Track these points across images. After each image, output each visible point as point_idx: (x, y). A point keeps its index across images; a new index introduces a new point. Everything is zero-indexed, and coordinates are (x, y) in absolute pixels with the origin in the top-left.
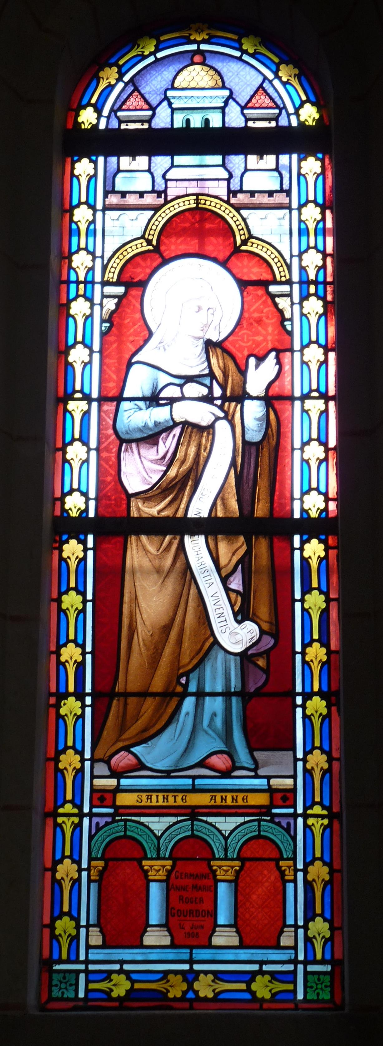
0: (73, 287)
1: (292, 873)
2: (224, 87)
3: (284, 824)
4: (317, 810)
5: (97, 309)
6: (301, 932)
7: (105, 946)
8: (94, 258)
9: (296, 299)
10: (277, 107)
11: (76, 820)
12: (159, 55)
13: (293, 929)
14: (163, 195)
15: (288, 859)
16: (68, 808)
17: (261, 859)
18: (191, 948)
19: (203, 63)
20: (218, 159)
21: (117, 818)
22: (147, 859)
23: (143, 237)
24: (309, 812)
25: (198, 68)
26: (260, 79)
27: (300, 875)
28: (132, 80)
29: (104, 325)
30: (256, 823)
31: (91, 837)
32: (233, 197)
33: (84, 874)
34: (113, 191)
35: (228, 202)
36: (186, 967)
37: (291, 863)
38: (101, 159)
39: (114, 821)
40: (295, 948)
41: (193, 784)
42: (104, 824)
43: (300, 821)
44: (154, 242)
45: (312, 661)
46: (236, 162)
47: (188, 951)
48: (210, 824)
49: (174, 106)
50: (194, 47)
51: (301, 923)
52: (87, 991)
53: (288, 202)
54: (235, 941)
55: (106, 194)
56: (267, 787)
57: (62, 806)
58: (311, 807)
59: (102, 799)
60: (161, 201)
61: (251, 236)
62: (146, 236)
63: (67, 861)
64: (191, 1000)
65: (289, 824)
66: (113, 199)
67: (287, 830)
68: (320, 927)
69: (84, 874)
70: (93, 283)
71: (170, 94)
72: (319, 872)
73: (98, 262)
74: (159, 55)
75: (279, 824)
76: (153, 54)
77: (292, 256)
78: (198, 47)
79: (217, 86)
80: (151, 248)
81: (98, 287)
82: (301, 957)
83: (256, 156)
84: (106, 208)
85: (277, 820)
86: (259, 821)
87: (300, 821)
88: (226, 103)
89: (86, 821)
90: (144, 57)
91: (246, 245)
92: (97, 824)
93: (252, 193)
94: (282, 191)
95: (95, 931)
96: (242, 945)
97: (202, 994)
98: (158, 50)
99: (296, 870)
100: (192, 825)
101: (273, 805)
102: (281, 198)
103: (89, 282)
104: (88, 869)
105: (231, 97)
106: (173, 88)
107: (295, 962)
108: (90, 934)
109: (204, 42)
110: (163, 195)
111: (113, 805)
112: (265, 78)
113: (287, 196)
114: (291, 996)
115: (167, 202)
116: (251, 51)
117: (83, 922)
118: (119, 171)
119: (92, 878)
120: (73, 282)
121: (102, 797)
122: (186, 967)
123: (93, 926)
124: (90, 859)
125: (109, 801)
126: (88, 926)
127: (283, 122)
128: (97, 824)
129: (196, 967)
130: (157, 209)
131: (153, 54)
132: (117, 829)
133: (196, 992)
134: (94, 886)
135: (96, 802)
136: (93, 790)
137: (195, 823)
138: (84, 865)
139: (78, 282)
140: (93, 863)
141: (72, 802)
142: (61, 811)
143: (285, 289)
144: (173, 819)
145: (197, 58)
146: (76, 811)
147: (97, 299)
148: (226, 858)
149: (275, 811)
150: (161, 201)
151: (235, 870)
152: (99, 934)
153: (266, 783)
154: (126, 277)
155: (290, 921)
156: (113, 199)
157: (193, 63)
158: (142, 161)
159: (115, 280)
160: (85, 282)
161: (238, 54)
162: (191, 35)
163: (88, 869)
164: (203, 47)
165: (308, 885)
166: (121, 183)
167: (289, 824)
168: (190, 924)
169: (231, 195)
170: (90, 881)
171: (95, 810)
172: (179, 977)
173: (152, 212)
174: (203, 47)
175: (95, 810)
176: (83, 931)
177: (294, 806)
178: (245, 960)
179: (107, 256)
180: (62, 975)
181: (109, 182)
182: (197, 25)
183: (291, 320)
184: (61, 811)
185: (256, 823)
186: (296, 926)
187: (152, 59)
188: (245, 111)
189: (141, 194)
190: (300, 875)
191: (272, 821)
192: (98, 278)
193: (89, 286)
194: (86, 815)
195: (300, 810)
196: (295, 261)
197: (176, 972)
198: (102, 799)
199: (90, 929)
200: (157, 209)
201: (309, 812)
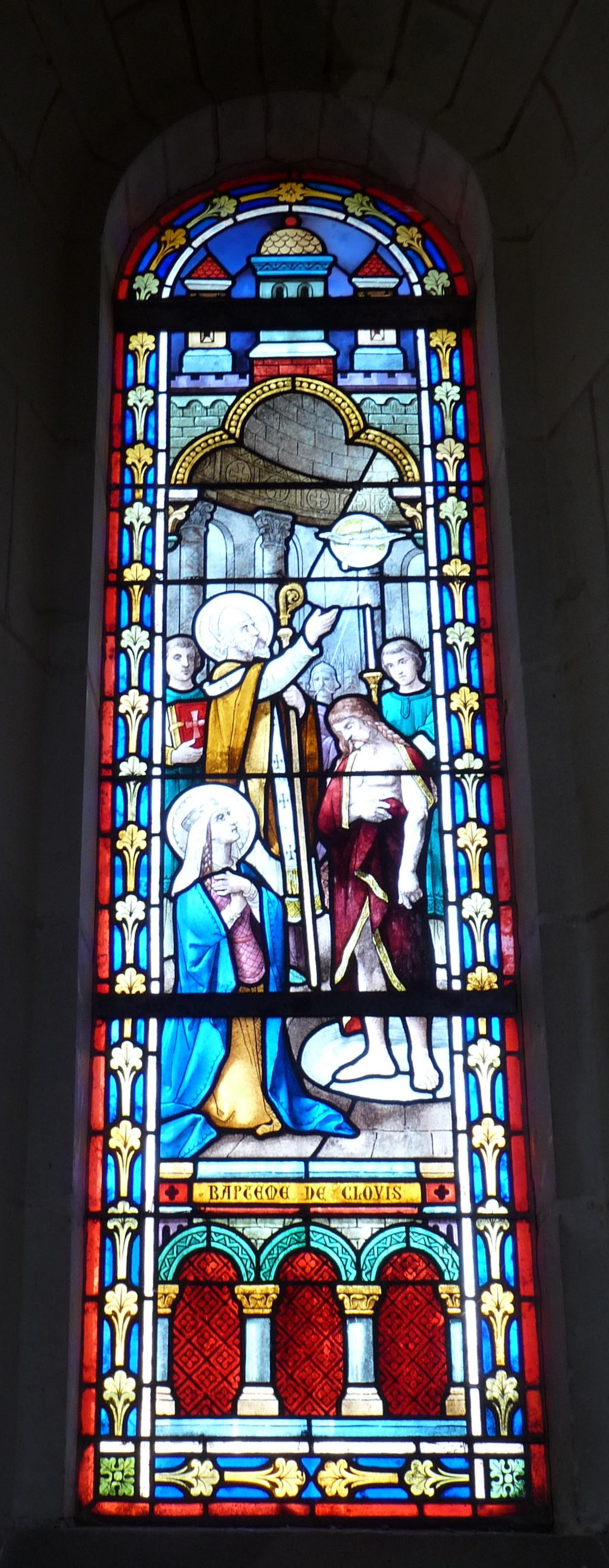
0: (128, 493)
1: (458, 1303)
2: (325, 252)
3: (443, 1228)
4: (492, 1207)
5: (160, 517)
6: (475, 1394)
7: (181, 1413)
8: (156, 451)
9: (430, 500)
10: (394, 275)
11: (133, 1224)
12: (240, 217)
13: (462, 1390)
14: (248, 376)
15: (451, 1282)
16: (123, 1207)
17: (411, 1300)
18: (309, 1418)
19: (298, 226)
20: (319, 334)
21: (195, 1221)
22: (240, 1281)
23: (222, 428)
24: (481, 1210)
25: (291, 232)
26: (372, 244)
27: (470, 1306)
28: (205, 244)
29: (170, 538)
30: (403, 1229)
31: (158, 1251)
32: (342, 377)
33: (148, 1306)
34: (181, 373)
35: (334, 383)
36: (304, 1447)
37: (456, 1289)
38: (164, 336)
39: (191, 1225)
40: (467, 1417)
41: (307, 1171)
42: (176, 1230)
43: (467, 1223)
44: (237, 436)
45: (477, 1066)
46: (344, 339)
47: (305, 1422)
48: (334, 1230)
49: (259, 273)
50: (285, 208)
51: (474, 1379)
52: (154, 1484)
53: (415, 383)
54: (377, 1408)
55: (171, 376)
56: (414, 1176)
57: (114, 1204)
58: (483, 1203)
59: (172, 1193)
60: (245, 383)
61: (367, 426)
62: (227, 427)
63: (121, 1288)
64: (311, 1502)
65: (450, 1229)
66: (183, 382)
67: (448, 1238)
68: (503, 1387)
69: (148, 1306)
70: (155, 486)
71: (254, 260)
72: (498, 1301)
73: (162, 457)
74: (240, 217)
75: (435, 1230)
76: (233, 216)
77: (422, 446)
78: (290, 208)
79: (316, 252)
80: (232, 442)
81: (161, 492)
82: (477, 1431)
83: (368, 332)
84: (172, 392)
85: (431, 1224)
86: (408, 1226)
87: (467, 1223)
88: (329, 270)
89: (149, 1222)
90: (220, 219)
91: (359, 438)
92: (166, 1230)
93: (367, 373)
94: (405, 370)
95: (163, 1392)
96: (388, 1414)
97: (330, 1492)
98: (239, 211)
99: (463, 1298)
100: (307, 1232)
101: (424, 1203)
102: (403, 380)
103: (151, 486)
104: (155, 1299)
105: (335, 263)
106: (258, 254)
107: (469, 1440)
108: (158, 1397)
109: (298, 203)
110: (248, 376)
111: (189, 1202)
112: (378, 243)
113: (412, 377)
114: (464, 1493)
115: (252, 384)
116: (359, 214)
117: (147, 1378)
118: (187, 348)
119: (160, 1311)
120: (128, 486)
121: (170, 1189)
122: (304, 1447)
123: (162, 1384)
124: (157, 1281)
125: (182, 1195)
126: (154, 1385)
127: (404, 291)
128: (166, 1230)
129: (320, 1448)
130: (239, 393)
131: (233, 216)
132: (195, 1237)
133: (321, 1489)
134: (163, 1324)
135: (164, 1198)
136: (159, 1181)
137: (312, 1228)
138: (148, 1291)
139: (134, 487)
140: (161, 1289)
141: (129, 1199)
142: (111, 1210)
143: (416, 492)
144: (279, 1223)
145: (290, 221)
146: (135, 1210)
147: (160, 504)
148: (358, 1281)
149: (427, 1210)
150: (245, 383)
151: (373, 1300)
152: (170, 1398)
153: (414, 1170)
154: (198, 478)
155: (458, 1376)
156: (183, 382)
157: (284, 227)
158: (220, 338)
159: (185, 482)
160: (145, 486)
161: (342, 216)
162: (279, 195)
163: (155, 1299)
164: (295, 209)
165: (485, 1321)
166: (192, 362)
167: (450, 1229)
168: (308, 1387)
169: (339, 375)
170: (156, 1316)
171: (162, 1209)
172: (293, 1464)
173: (234, 397)
174: (295, 209)
175: (162, 1209)
176: (146, 1392)
177: (456, 1203)
178: (394, 1438)
179: (174, 453)
180: (113, 1460)
181: (175, 362)
182: (289, 185)
183: (424, 530)
184: (111, 1210)
185: (403, 1229)
186: (465, 1384)
187: (230, 222)
188: (354, 280)
189: (219, 376)
190: (470, 1306)
191: (425, 1226)
192: (161, 480)
193: (150, 492)
194: (149, 1215)
195: (466, 1207)
196: (427, 452)
197: (288, 1457)
198: (172, 1193)
199: (159, 1389)
200: (239, 393)
201: (481, 1210)
